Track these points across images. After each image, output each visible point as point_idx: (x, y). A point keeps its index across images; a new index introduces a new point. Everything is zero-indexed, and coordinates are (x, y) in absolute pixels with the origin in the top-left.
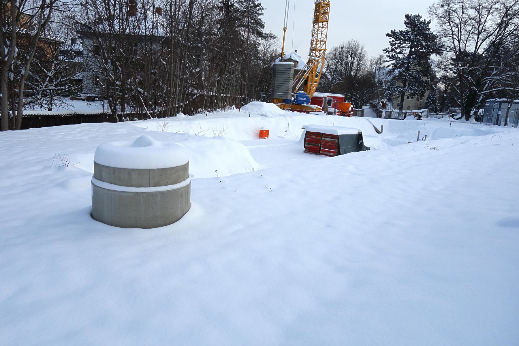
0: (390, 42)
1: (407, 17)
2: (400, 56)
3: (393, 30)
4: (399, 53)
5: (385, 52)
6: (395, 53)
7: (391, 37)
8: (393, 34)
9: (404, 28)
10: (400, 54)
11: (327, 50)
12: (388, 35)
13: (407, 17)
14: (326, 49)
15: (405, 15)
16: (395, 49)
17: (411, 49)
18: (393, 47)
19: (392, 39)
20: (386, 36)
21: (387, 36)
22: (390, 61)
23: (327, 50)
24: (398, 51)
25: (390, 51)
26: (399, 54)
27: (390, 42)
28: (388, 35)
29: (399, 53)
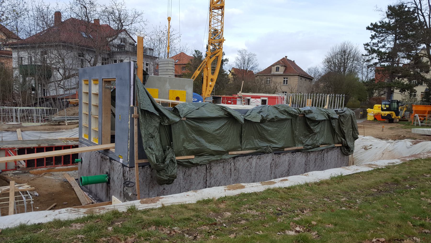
0: (372, 35)
1: (390, 8)
2: (383, 50)
3: (372, 22)
4: (384, 47)
5: (366, 46)
6: (378, 48)
7: (372, 31)
8: (374, 27)
9: (387, 20)
10: (384, 48)
11: (225, 40)
12: (368, 28)
13: (390, 8)
14: (224, 39)
15: (387, 6)
16: (378, 43)
17: (395, 43)
18: (375, 41)
19: (373, 33)
20: (366, 29)
21: (367, 29)
22: (370, 54)
23: (225, 40)
24: (380, 45)
25: (372, 45)
26: (383, 48)
27: (372, 35)
28: (368, 28)
29: (384, 47)
